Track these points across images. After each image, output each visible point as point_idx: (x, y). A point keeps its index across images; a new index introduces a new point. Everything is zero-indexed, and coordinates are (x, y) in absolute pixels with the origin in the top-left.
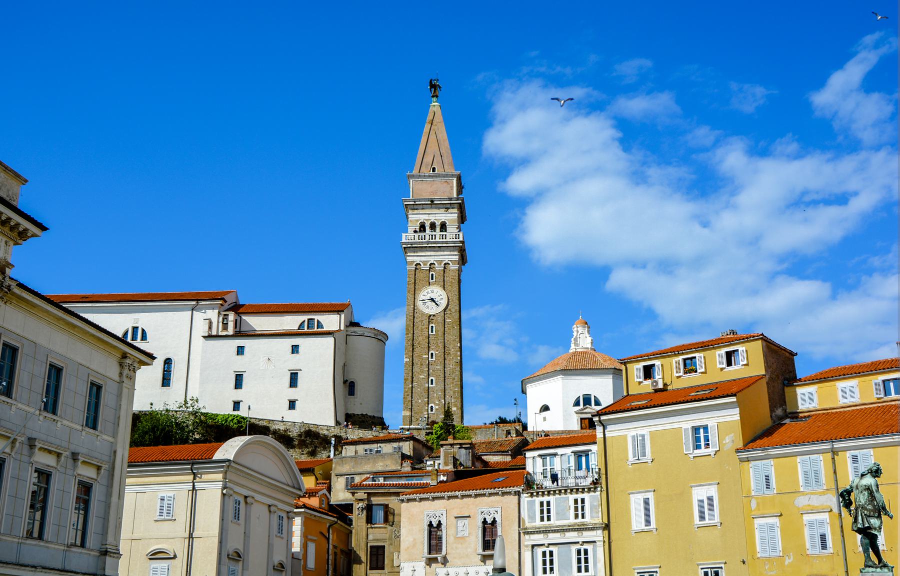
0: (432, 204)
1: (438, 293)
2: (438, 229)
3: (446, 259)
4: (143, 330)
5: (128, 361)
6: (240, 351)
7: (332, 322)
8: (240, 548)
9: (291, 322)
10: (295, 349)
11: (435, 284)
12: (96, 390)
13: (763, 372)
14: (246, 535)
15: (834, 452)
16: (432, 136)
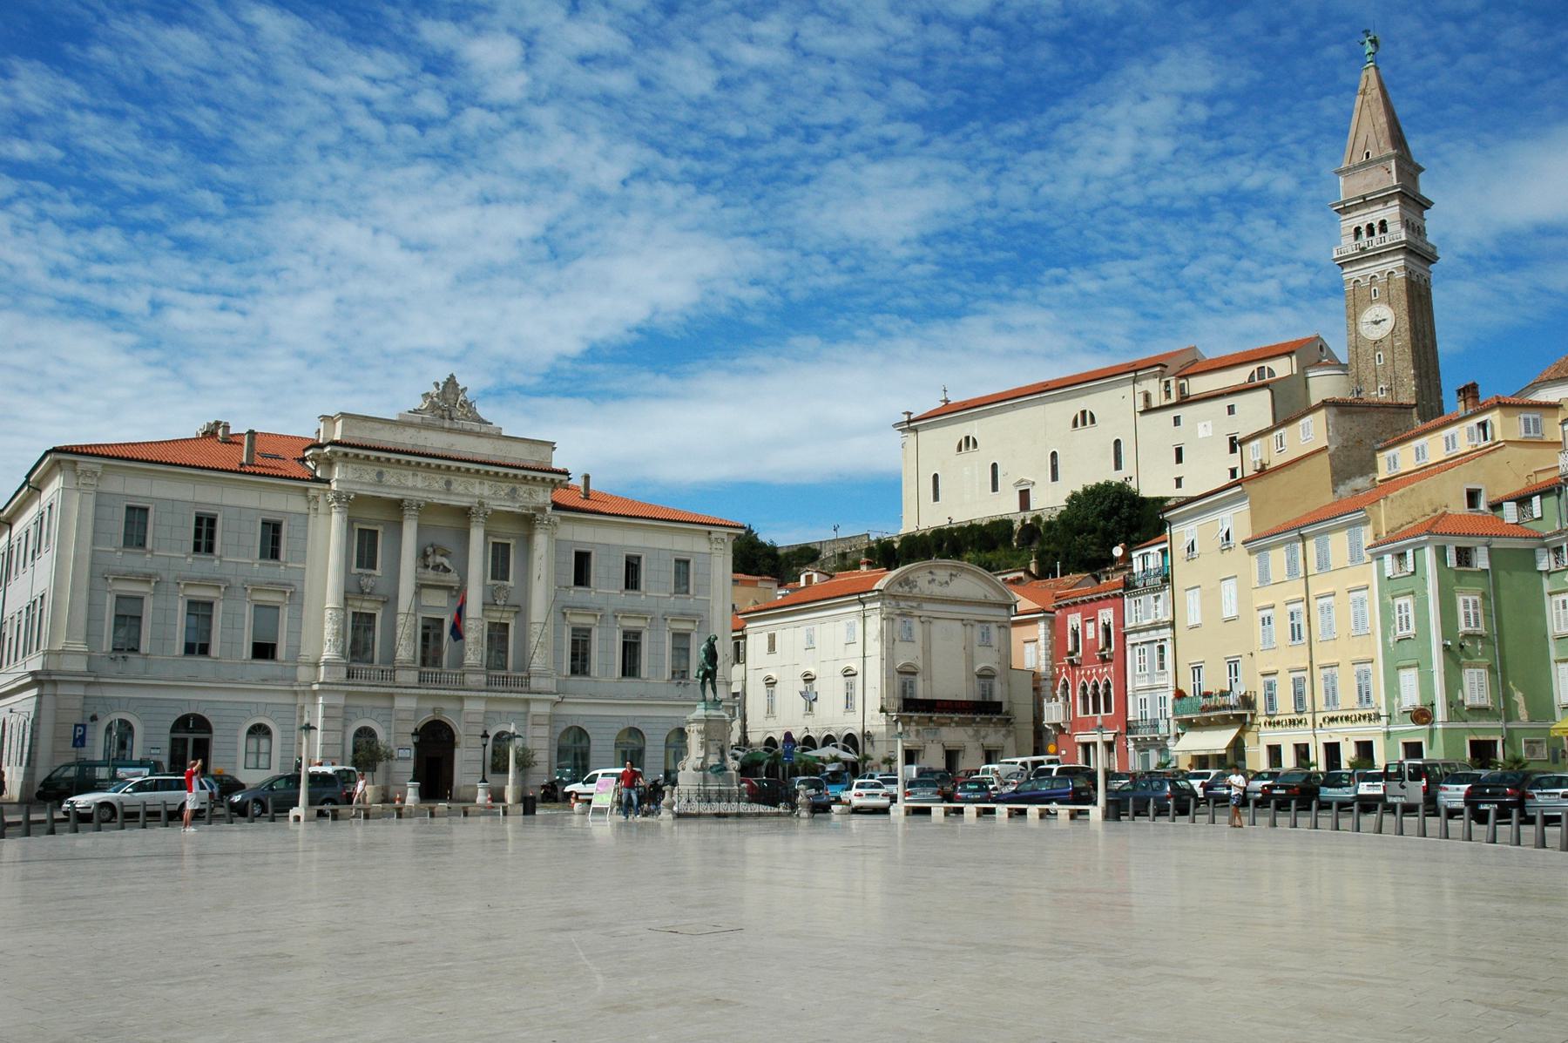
0: (1365, 202)
1: (1383, 311)
2: (1364, 234)
3: (1390, 267)
4: (1092, 415)
5: (713, 536)
6: (1177, 421)
7: (1282, 368)
8: (920, 664)
9: (1240, 376)
10: (1231, 410)
11: (1378, 301)
12: (682, 565)
13: (1326, 443)
14: (927, 651)
15: (1303, 538)
16: (1366, 112)
